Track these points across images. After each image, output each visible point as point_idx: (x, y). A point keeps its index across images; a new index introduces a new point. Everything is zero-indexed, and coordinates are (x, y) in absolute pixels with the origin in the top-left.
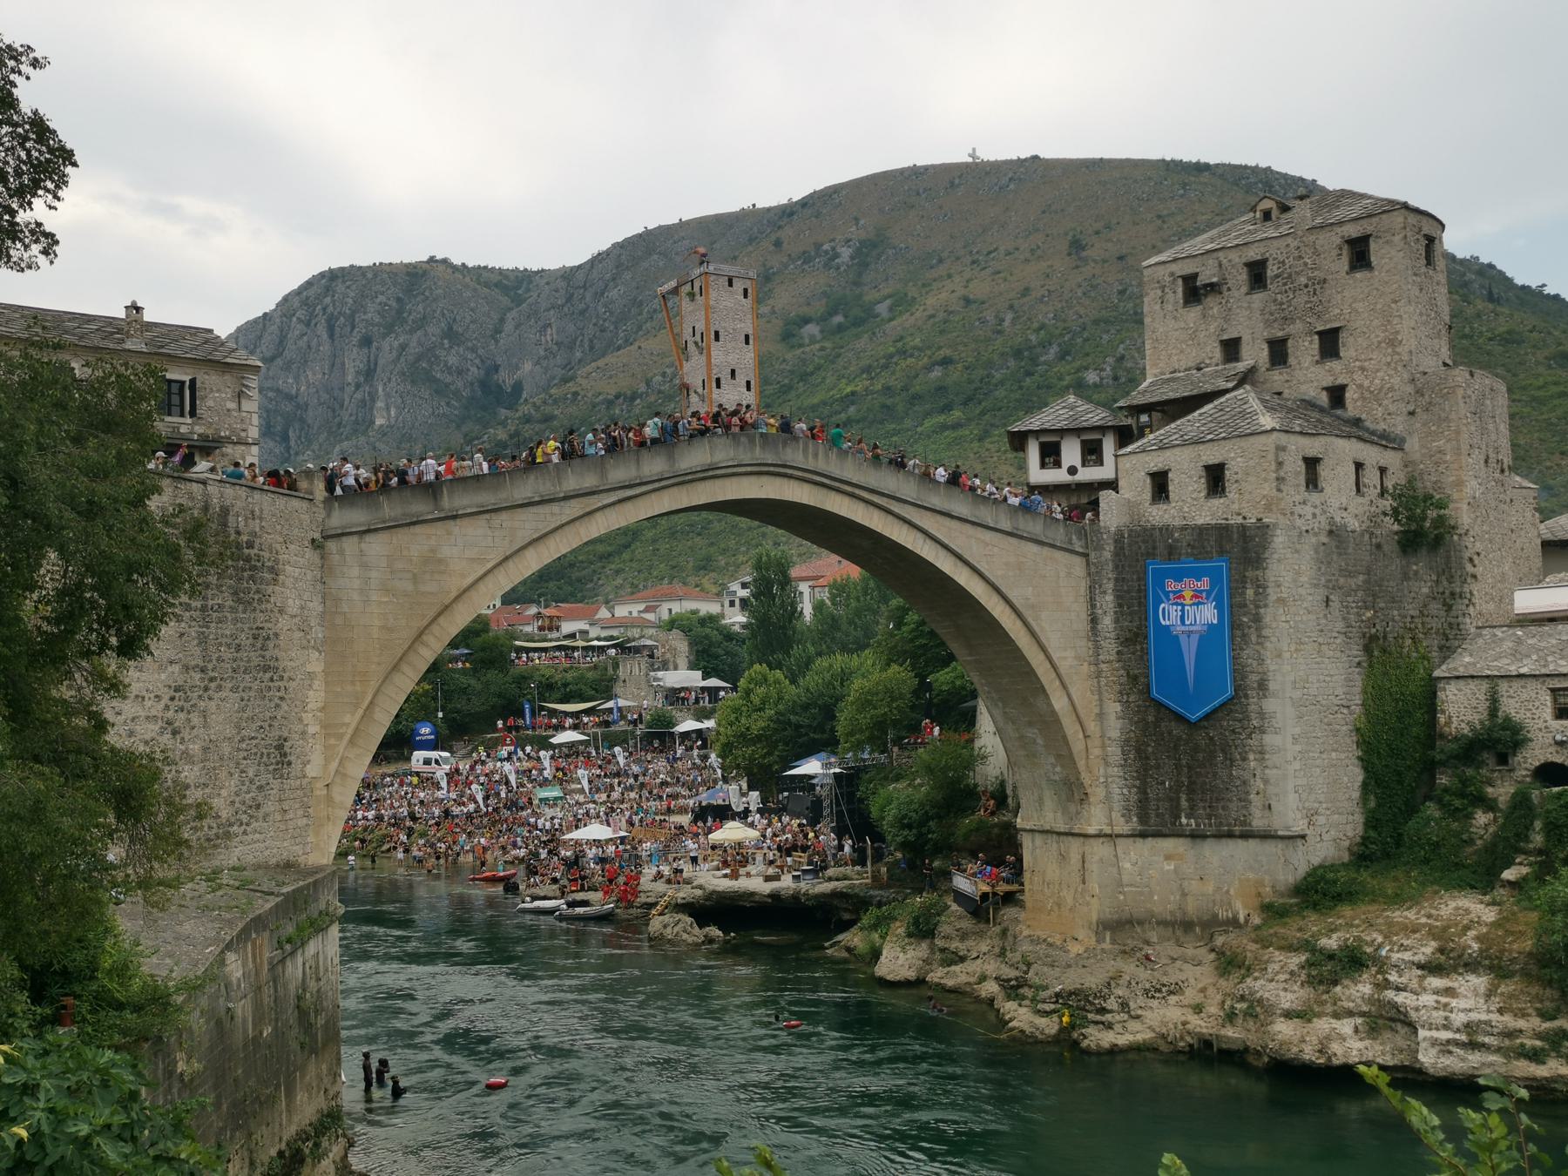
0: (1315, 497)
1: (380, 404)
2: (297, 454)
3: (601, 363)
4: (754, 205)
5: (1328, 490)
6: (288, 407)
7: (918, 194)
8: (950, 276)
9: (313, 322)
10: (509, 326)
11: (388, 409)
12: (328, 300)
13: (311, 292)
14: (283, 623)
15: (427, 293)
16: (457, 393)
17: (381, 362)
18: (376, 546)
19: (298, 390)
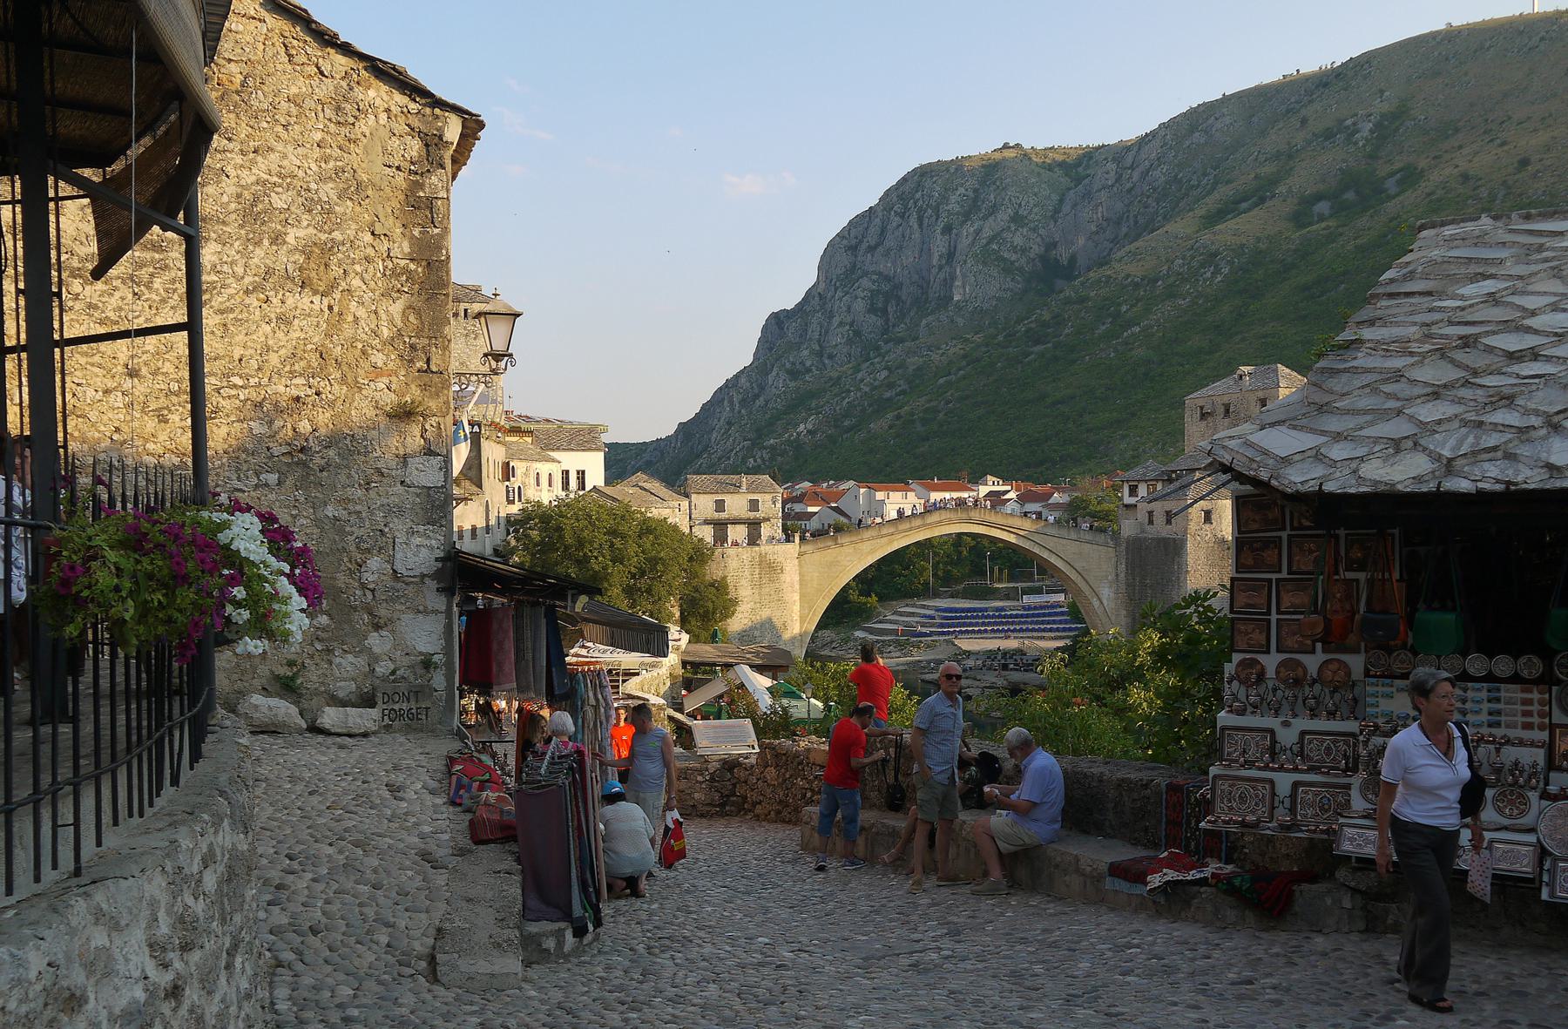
0: (1207, 526)
1: (958, 283)
2: (894, 326)
3: (1132, 247)
4: (1298, 71)
5: (1214, 524)
6: (886, 287)
7: (1447, 59)
8: (1460, 147)
9: (907, 214)
10: (1066, 208)
11: (964, 288)
12: (918, 195)
13: (907, 188)
14: (785, 586)
15: (998, 184)
16: (1020, 269)
17: (959, 247)
18: (817, 556)
19: (895, 272)
